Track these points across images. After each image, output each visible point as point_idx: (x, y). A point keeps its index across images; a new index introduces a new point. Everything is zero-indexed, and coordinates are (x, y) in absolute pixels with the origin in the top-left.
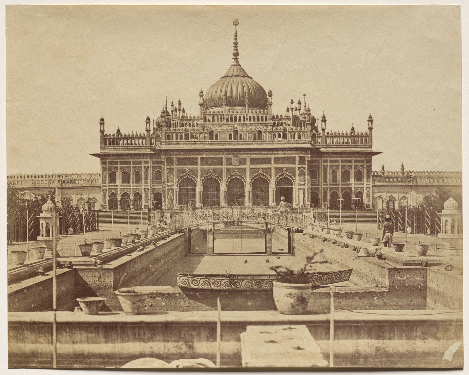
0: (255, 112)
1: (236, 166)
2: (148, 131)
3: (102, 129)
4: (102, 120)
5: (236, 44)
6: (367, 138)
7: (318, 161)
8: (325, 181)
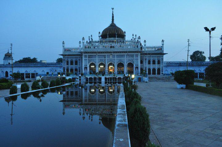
2: (80, 46)
4: (63, 42)
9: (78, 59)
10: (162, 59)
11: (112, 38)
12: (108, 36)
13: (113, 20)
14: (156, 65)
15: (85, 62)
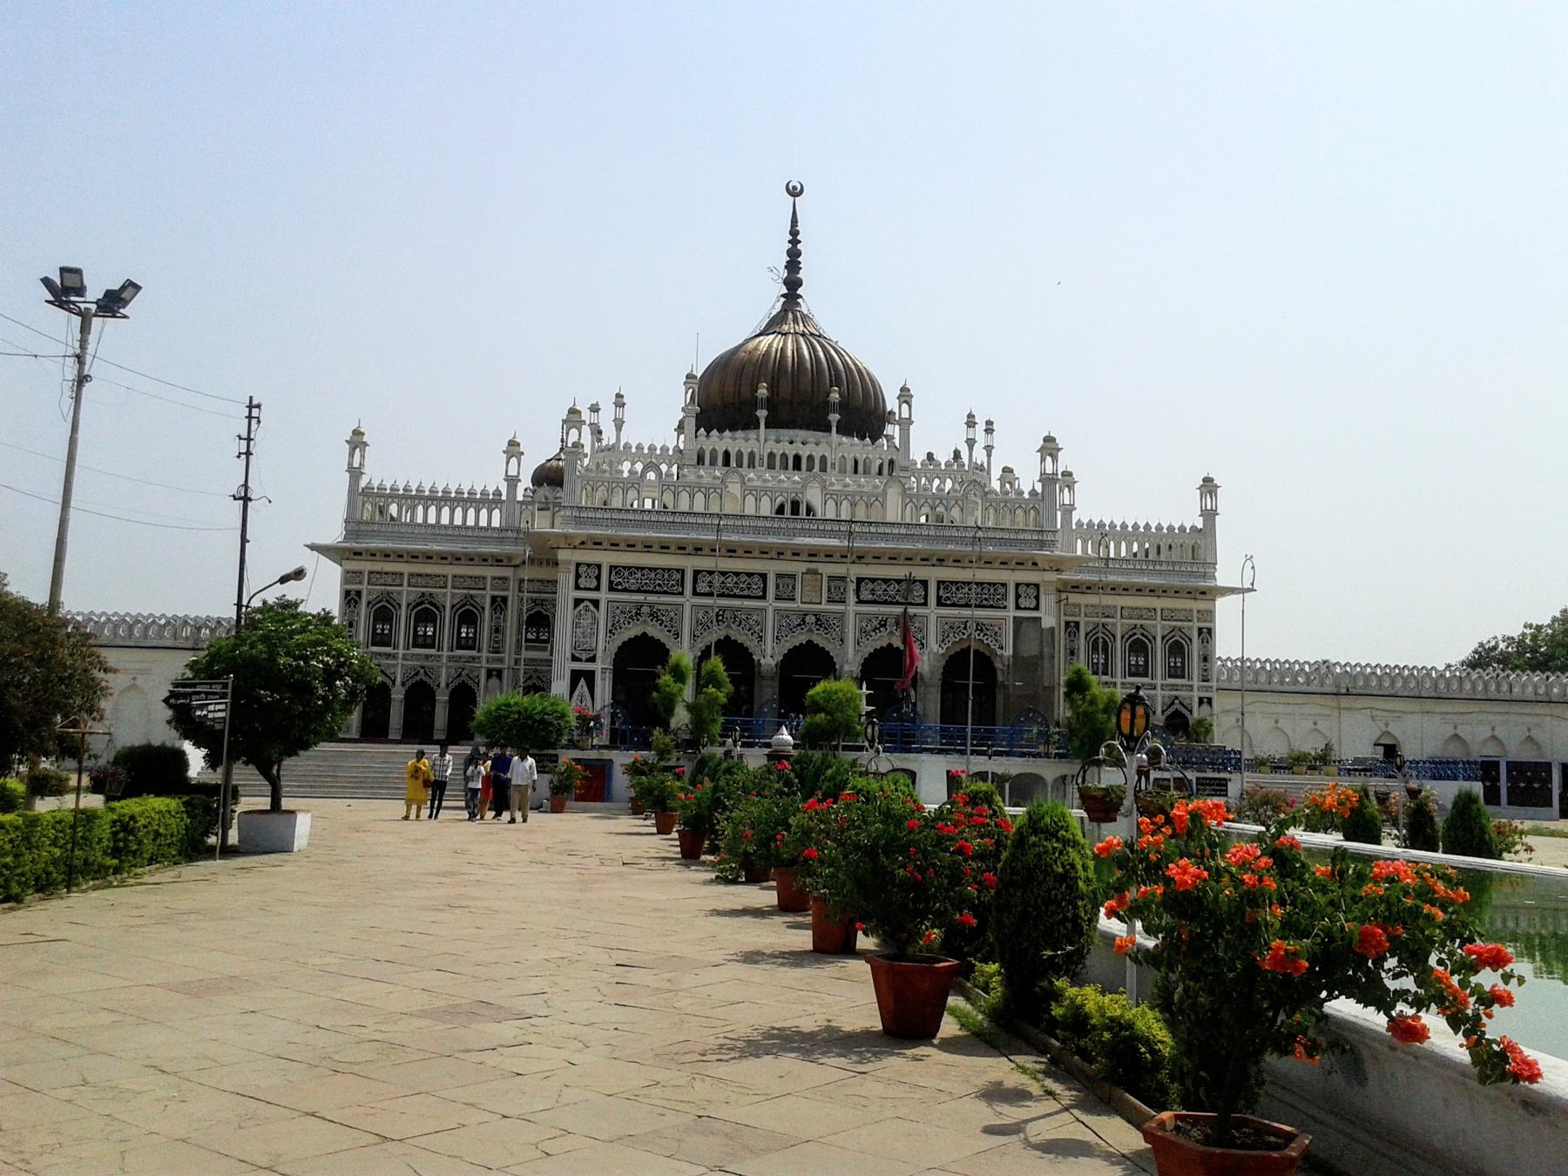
0: (853, 447)
2: (512, 481)
3: (356, 464)
4: (357, 433)
9: (489, 593)
10: (1207, 634)
11: (802, 434)
12: (762, 414)
13: (793, 285)
14: (1159, 682)
15: (576, 625)
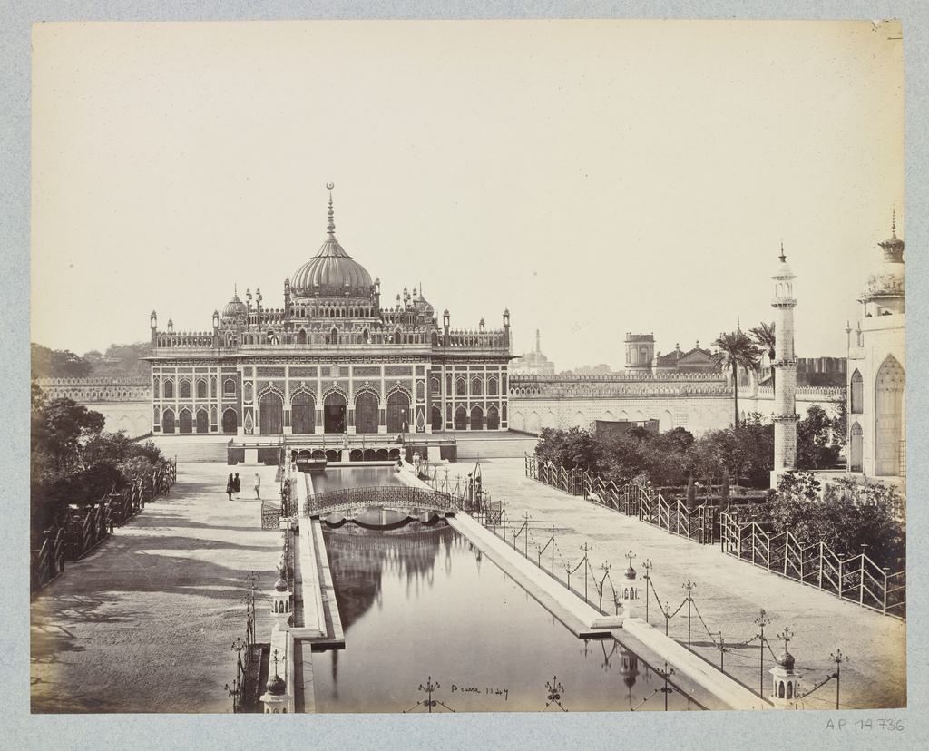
1: (335, 377)
5: (331, 213)
6: (504, 339)
7: (439, 369)
8: (449, 393)
13: (331, 228)
